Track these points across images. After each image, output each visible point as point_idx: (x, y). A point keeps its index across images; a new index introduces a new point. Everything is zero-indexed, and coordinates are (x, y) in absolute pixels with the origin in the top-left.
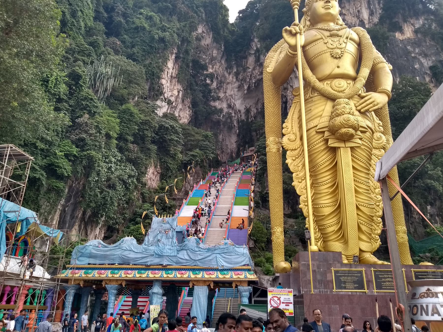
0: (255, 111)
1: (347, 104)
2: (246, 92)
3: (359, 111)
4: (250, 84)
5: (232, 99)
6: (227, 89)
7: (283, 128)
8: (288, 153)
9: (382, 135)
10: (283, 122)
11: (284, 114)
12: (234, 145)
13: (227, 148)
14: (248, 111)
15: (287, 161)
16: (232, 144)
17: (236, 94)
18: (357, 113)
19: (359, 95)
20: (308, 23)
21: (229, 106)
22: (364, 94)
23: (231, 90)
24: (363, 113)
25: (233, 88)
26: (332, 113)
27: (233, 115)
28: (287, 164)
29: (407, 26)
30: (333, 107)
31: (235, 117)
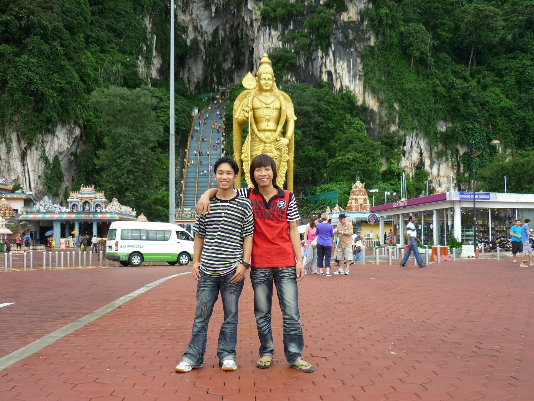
0: (223, 35)
1: (270, 147)
2: (213, 15)
3: (275, 148)
4: (217, 6)
5: (198, 20)
6: (193, 8)
7: (242, 150)
8: (244, 163)
9: (287, 155)
10: (242, 146)
11: (243, 143)
12: (201, 72)
13: (194, 76)
14: (215, 33)
15: (243, 168)
16: (199, 70)
17: (202, 13)
18: (275, 150)
19: (276, 140)
20: (257, 88)
21: (195, 28)
22: (278, 139)
23: (198, 10)
24: (278, 149)
25: (199, 7)
26: (263, 150)
27: (200, 38)
28: (243, 169)
29: (352, 7)
30: (264, 147)
31: (201, 41)
